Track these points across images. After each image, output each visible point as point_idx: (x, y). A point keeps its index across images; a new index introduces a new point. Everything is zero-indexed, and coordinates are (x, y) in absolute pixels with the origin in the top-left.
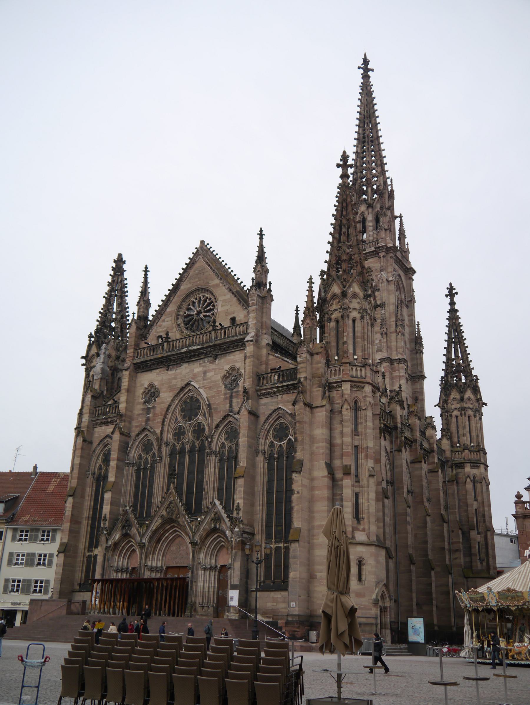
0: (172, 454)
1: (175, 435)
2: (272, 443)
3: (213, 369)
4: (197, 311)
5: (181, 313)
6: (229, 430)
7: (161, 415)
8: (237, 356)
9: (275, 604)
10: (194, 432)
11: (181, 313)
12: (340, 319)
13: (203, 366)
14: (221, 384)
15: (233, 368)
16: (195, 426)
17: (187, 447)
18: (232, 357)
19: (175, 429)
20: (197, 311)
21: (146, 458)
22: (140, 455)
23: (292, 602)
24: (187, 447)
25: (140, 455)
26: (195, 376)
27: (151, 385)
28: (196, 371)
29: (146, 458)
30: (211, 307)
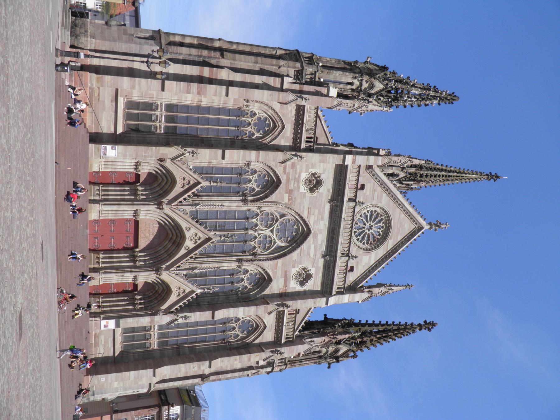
2: (239, 320)
4: (372, 226)
5: (377, 209)
7: (289, 200)
9: (103, 343)
10: (266, 237)
11: (377, 209)
12: (320, 354)
13: (321, 245)
14: (300, 266)
16: (270, 237)
20: (372, 226)
21: (250, 181)
22: (255, 172)
23: (106, 379)
25: (255, 172)
26: (316, 235)
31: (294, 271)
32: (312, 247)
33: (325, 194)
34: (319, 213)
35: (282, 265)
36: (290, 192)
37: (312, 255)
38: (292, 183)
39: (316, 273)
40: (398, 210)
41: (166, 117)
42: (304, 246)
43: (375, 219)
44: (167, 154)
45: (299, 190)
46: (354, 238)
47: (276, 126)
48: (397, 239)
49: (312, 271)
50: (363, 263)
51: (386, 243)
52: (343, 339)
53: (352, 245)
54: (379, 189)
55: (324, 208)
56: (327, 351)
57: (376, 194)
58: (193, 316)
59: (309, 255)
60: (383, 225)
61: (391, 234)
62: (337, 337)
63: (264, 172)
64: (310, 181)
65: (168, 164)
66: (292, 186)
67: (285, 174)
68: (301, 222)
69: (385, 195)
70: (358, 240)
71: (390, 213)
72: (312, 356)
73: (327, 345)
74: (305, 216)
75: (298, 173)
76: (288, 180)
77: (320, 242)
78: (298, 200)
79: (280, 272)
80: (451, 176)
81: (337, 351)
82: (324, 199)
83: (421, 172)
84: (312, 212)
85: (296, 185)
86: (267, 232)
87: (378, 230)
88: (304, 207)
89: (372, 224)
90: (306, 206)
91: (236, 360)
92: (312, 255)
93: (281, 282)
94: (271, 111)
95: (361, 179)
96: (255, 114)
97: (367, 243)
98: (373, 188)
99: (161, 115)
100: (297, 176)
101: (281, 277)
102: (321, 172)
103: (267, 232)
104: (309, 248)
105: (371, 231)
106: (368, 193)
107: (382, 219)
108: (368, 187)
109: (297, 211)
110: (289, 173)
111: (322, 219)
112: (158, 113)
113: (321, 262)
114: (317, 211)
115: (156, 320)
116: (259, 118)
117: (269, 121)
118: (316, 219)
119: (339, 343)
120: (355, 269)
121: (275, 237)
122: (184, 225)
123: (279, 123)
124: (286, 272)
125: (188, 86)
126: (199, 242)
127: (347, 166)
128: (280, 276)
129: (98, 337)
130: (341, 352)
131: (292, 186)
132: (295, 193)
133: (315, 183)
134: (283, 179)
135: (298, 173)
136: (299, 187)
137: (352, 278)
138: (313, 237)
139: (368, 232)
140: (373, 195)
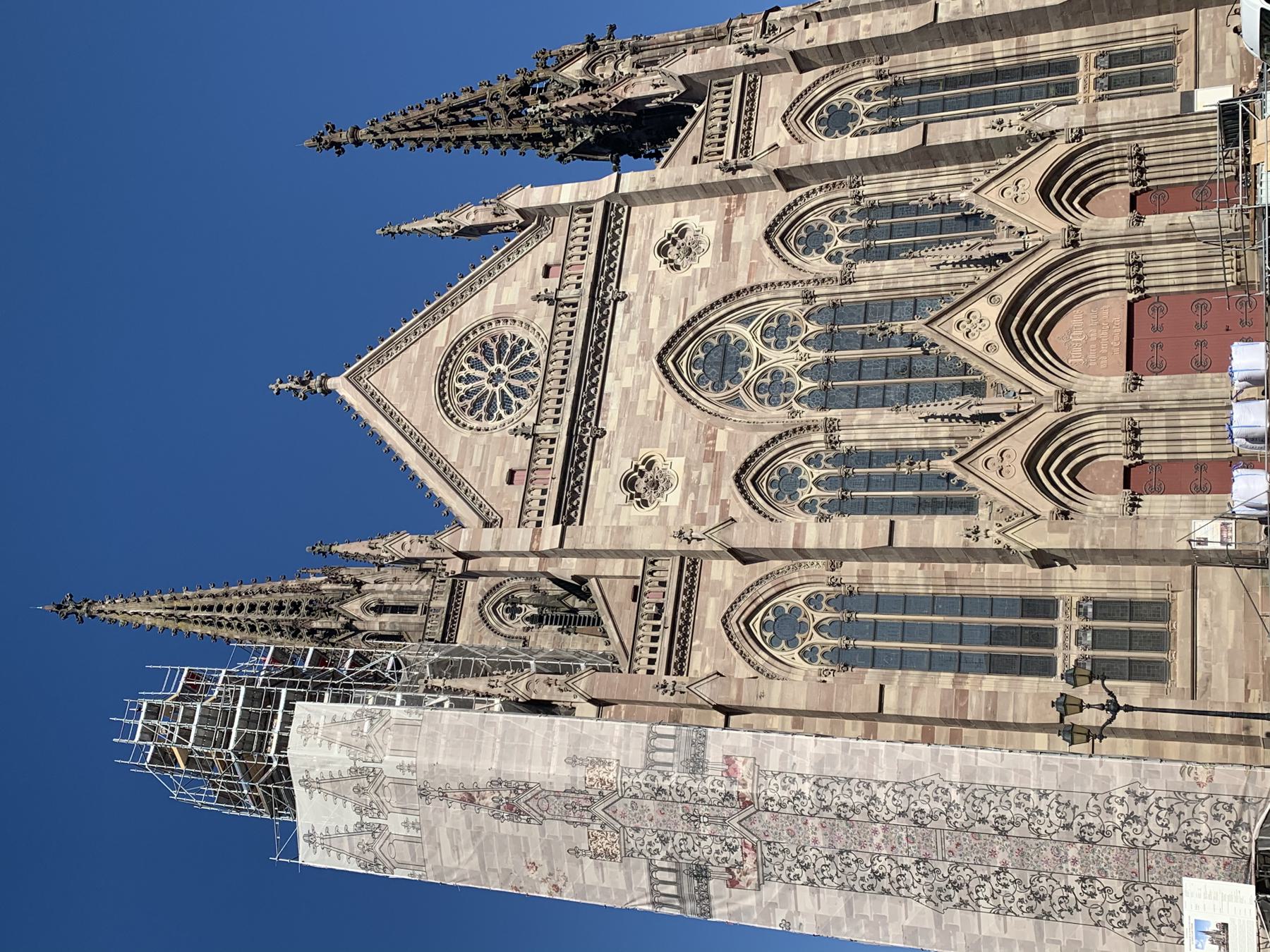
0: (824, 399)
1: (773, 402)
3: (646, 301)
5: (476, 424)
6: (801, 247)
7: (714, 437)
8: (637, 242)
10: (779, 345)
11: (476, 424)
12: (636, 57)
14: (689, 273)
15: (662, 250)
17: (819, 355)
18: (635, 252)
19: (761, 401)
20: (490, 381)
24: (819, 355)
26: (644, 350)
27: (628, 483)
28: (633, 346)
29: (817, 483)
30: (493, 346)
31: (705, 261)
32: (653, 323)
33: (618, 453)
34: (634, 405)
35: (735, 276)
36: (711, 456)
37: (656, 301)
38: (704, 480)
39: (643, 257)
40: (416, 421)
41: (1053, 645)
42: (675, 324)
43: (480, 400)
44: (1051, 530)
45: (687, 461)
46: (539, 348)
47: (746, 623)
48: (422, 349)
49: (655, 261)
50: (517, 285)
51: (454, 337)
52: (576, 94)
53: (548, 331)
54: (467, 474)
55: (620, 420)
56: (616, 67)
57: (477, 461)
58: (981, 130)
59: (662, 298)
60: (458, 385)
61: (439, 360)
62: (591, 99)
63: (780, 505)
64: (655, 485)
65: (1045, 507)
66: (706, 471)
67: (724, 501)
68: (682, 383)
69: (453, 459)
70: (530, 346)
71: (439, 414)
72: (658, 52)
73: (616, 80)
74: (672, 399)
75: (689, 504)
76: (716, 486)
77: (634, 335)
78: (688, 436)
79: (743, 257)
80: (204, 608)
81: (590, 67)
82: (620, 441)
83: (294, 616)
84: (652, 408)
85: (695, 474)
86: (774, 357)
87: (472, 372)
88: (674, 421)
89: (490, 387)
90: (668, 422)
91: (868, 28)
92: (656, 301)
93: (738, 234)
94: (761, 661)
95: (518, 497)
96: (803, 654)
97: (504, 337)
98: (483, 475)
99: (1066, 647)
100: (691, 497)
101: (739, 244)
102: (625, 510)
103: (774, 357)
104: (663, 318)
105: (492, 369)
106: (499, 461)
107: (461, 399)
108: (499, 476)
109: (693, 408)
110: (712, 503)
111: (626, 392)
112: (1075, 653)
113: (630, 284)
114: (640, 411)
115: (1083, 117)
116: (792, 643)
117: (764, 638)
118: (642, 391)
119: (586, 86)
120: (540, 270)
121: (754, 346)
122: (1003, 356)
123: (737, 630)
124: (726, 258)
125: (994, 712)
126: (962, 315)
127: (556, 522)
128: (743, 248)
129: (1242, 73)
130: (580, 63)
131: (706, 471)
132: (696, 454)
133: (640, 483)
134: (728, 488)
135: (689, 504)
136: (688, 468)
137: (550, 250)
138: (652, 346)
139: (501, 366)
140: (484, 458)
